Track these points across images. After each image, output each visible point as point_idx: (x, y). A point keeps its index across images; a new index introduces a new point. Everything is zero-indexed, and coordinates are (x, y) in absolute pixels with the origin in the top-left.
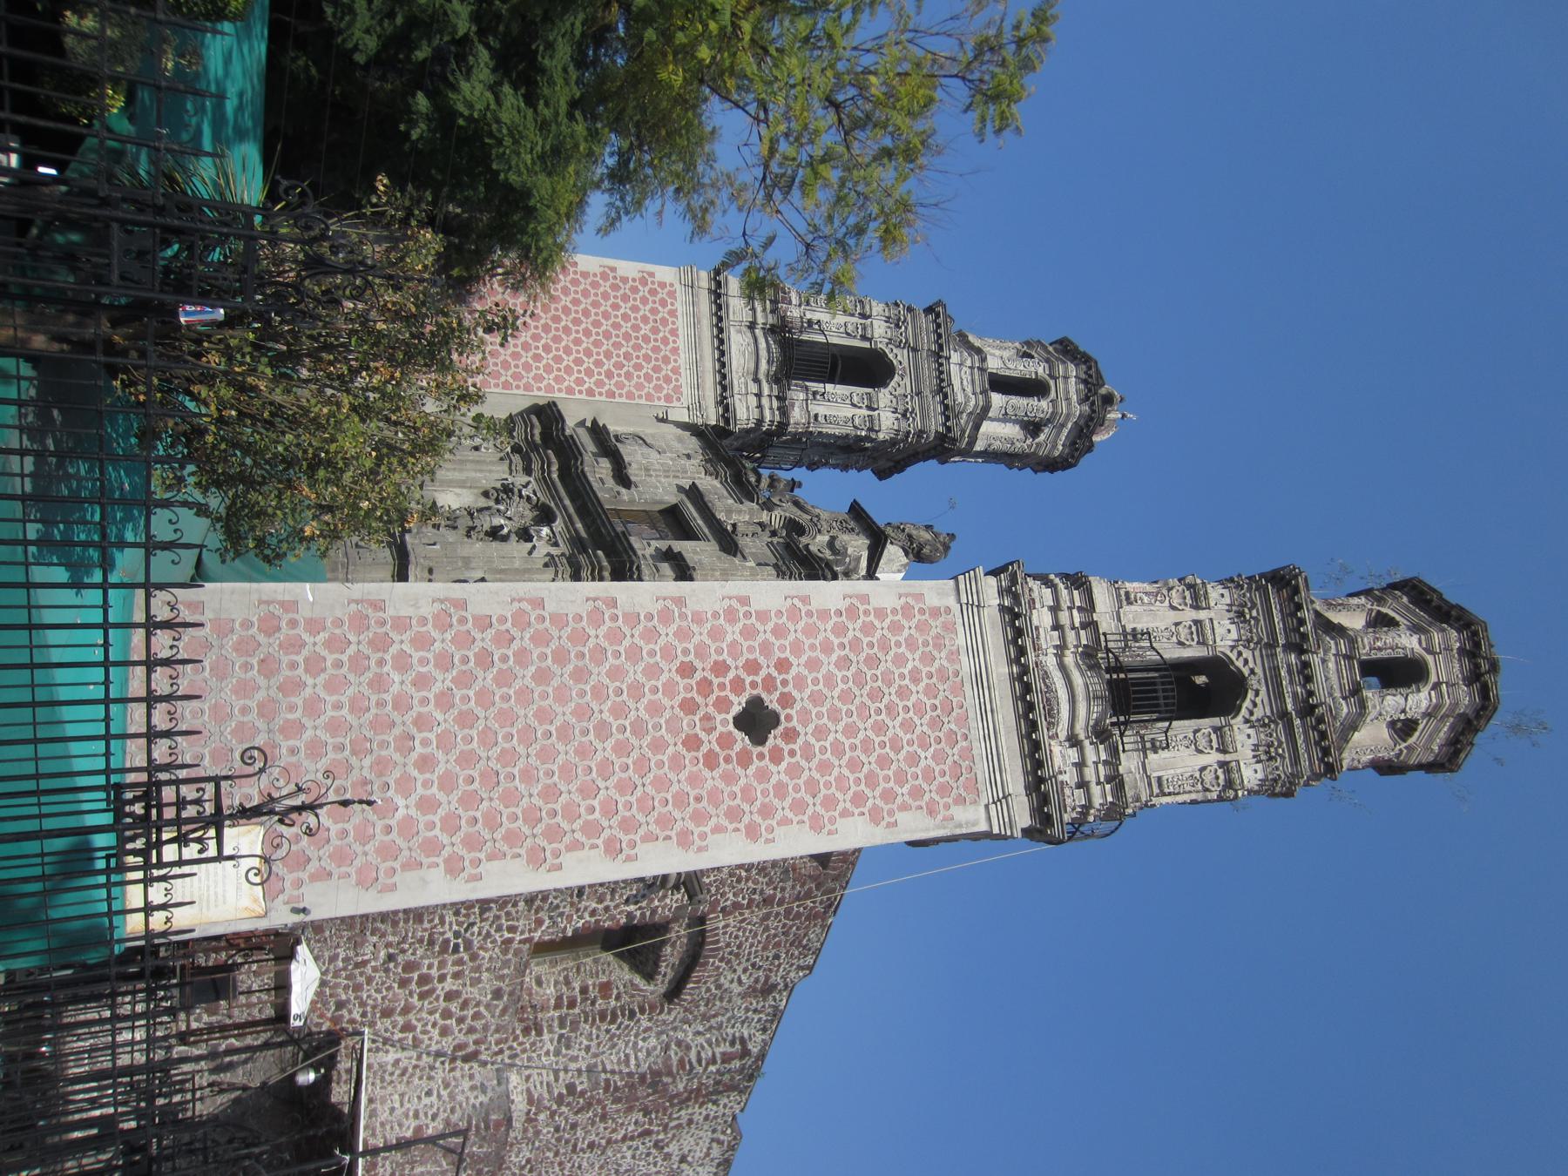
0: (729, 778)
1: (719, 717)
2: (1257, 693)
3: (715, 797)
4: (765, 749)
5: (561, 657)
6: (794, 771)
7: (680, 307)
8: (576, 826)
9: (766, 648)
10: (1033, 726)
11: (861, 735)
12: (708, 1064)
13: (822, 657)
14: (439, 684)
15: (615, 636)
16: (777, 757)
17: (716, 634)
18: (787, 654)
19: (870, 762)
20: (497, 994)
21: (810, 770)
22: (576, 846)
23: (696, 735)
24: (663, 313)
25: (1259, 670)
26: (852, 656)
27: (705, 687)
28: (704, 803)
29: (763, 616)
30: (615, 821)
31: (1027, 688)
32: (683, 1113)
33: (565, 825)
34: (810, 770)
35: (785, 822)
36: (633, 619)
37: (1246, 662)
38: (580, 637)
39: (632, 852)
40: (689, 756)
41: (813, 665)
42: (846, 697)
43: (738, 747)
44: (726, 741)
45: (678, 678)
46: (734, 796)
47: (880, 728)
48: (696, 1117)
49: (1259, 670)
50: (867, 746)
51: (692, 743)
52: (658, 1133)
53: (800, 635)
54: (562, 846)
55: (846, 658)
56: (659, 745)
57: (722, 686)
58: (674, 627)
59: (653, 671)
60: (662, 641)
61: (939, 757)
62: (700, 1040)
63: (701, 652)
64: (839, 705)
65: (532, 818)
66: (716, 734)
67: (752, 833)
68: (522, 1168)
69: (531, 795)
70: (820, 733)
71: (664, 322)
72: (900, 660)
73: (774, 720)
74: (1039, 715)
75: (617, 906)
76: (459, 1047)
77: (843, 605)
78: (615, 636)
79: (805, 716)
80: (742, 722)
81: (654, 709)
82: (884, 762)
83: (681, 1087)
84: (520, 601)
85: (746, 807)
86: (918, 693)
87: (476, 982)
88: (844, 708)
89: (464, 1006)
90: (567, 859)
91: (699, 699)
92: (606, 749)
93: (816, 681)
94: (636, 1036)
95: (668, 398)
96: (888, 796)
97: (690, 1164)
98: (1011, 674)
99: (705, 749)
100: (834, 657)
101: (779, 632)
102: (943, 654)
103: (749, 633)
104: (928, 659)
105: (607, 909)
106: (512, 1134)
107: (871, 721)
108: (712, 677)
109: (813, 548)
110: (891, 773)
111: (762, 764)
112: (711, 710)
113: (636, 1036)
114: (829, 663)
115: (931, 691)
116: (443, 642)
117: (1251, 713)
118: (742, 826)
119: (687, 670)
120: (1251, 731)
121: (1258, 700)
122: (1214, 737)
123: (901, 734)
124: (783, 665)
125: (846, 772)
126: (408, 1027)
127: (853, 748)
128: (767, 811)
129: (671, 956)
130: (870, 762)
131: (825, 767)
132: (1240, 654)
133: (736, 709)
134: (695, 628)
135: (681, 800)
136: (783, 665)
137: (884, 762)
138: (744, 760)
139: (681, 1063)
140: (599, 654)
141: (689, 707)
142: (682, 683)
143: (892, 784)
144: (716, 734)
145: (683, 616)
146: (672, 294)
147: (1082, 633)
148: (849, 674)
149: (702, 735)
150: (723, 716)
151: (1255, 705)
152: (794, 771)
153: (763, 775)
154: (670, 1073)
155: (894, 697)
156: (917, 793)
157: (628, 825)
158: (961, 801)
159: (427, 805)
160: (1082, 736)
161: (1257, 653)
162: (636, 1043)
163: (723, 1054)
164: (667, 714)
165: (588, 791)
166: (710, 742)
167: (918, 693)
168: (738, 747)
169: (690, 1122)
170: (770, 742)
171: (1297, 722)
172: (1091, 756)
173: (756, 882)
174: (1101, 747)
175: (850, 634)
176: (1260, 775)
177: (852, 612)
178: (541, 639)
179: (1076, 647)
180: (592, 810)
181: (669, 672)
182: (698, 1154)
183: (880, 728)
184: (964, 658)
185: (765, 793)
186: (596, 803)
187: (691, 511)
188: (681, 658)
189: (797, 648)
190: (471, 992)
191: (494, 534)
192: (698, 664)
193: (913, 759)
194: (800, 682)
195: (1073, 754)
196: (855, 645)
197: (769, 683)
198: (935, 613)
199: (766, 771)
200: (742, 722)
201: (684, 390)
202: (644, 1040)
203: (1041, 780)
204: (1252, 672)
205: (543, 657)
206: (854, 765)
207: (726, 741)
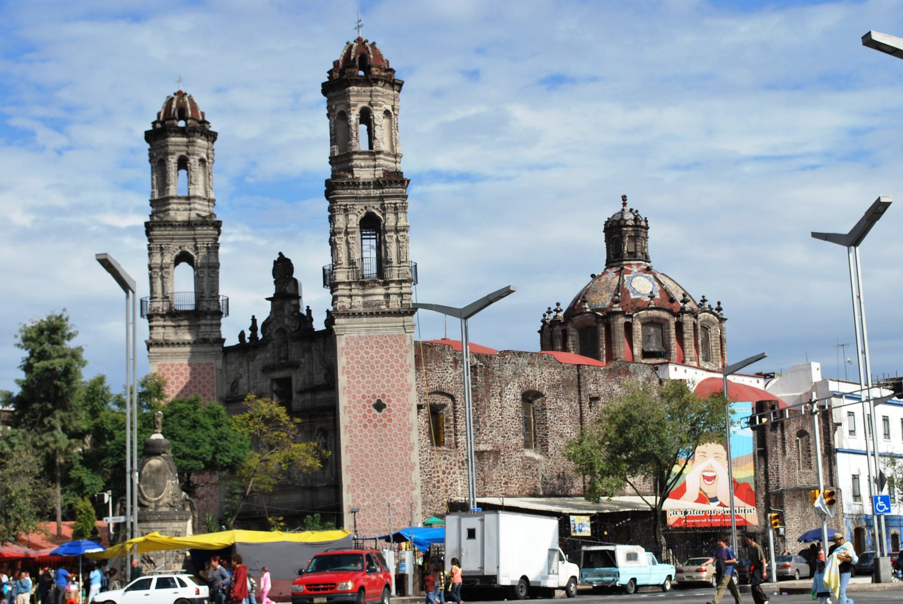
7: (169, 362)
9: (359, 402)
15: (356, 446)
16: (389, 401)
20: (445, 459)
21: (393, 391)
22: (410, 458)
24: (173, 370)
27: (370, 421)
29: (350, 402)
34: (393, 391)
35: (407, 400)
44: (385, 416)
50: (388, 372)
51: (385, 425)
56: (386, 435)
59: (366, 436)
63: (360, 422)
70: (383, 387)
71: (177, 370)
73: (379, 401)
76: (460, 468)
77: (346, 376)
79: (379, 391)
87: (440, 466)
89: (447, 468)
90: (413, 461)
92: (386, 450)
95: (212, 369)
109: (293, 330)
114: (363, 382)
119: (365, 426)
126: (451, 485)
128: (404, 405)
129: (439, 400)
131: (393, 386)
133: (376, 412)
138: (390, 411)
140: (361, 451)
146: (163, 365)
153: (394, 406)
157: (405, 444)
158: (405, 341)
159: (398, 495)
165: (397, 455)
166: (385, 420)
177: (348, 373)
181: (365, 431)
187: (278, 375)
190: (443, 467)
194: (369, 392)
198: (347, 343)
199: (393, 404)
201: (208, 361)
206: (393, 377)
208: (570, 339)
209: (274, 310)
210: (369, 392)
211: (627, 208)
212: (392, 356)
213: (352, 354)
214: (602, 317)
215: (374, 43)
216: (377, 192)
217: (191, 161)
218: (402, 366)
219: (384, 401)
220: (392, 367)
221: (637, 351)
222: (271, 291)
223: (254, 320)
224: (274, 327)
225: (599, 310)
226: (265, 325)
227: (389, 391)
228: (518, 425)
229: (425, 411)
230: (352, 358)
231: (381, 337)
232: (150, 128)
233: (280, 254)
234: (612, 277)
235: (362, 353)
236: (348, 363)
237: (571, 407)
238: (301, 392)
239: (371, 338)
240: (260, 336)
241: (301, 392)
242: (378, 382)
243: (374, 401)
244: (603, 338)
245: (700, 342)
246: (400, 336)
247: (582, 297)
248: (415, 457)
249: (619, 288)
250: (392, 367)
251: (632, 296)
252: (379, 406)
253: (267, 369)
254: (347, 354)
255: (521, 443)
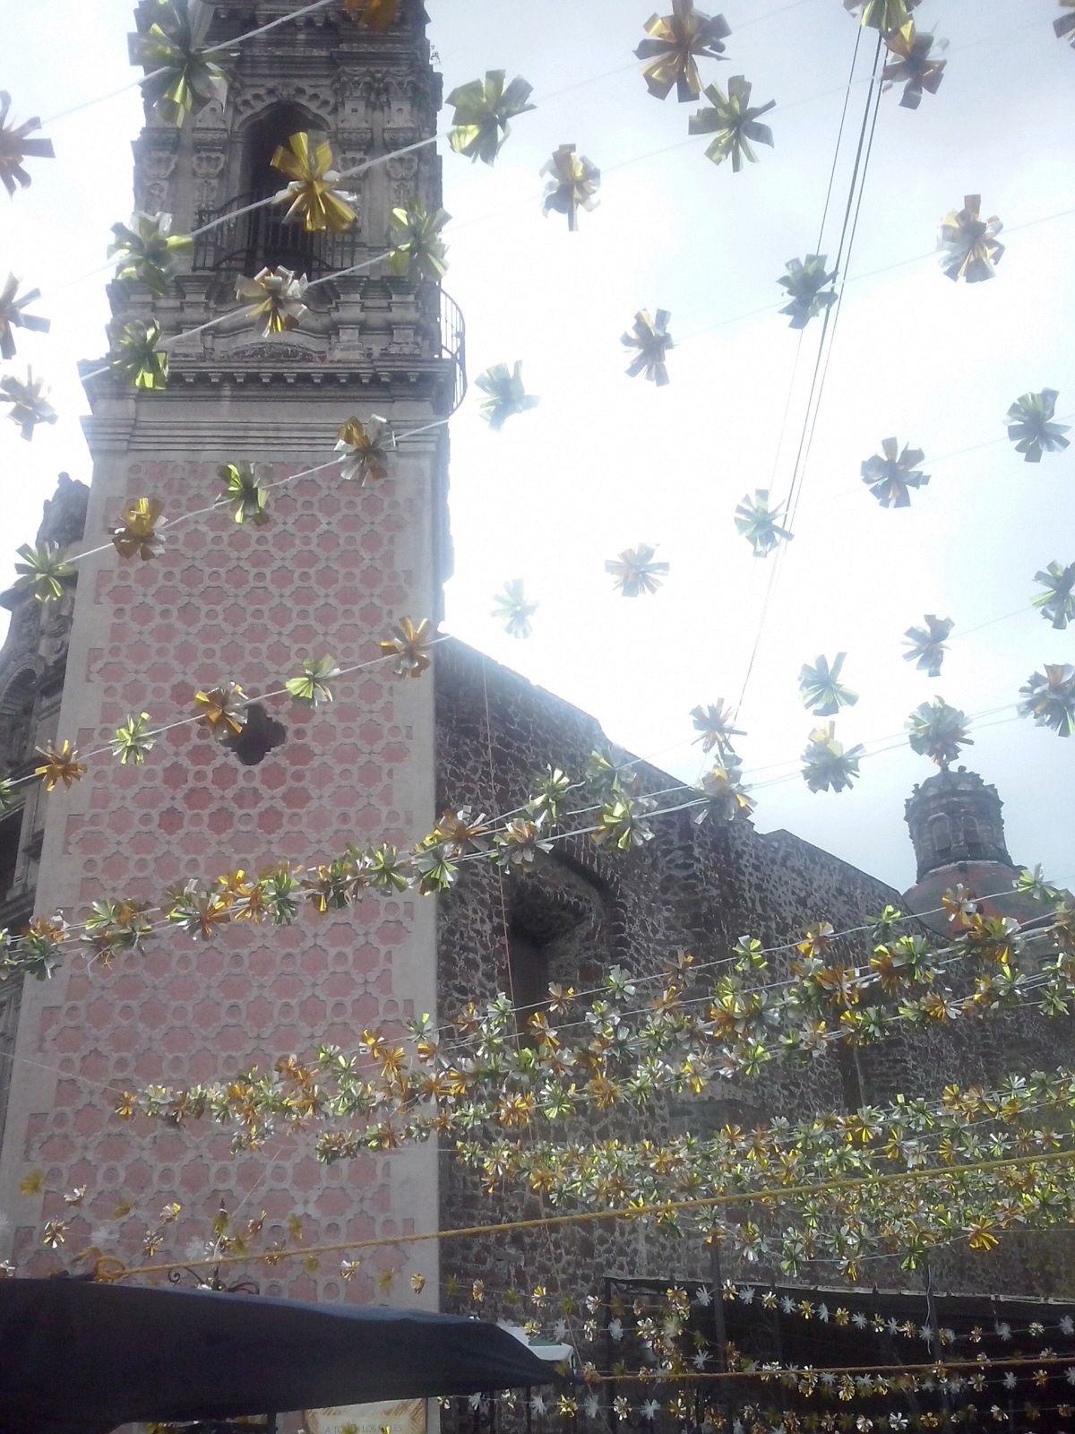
0: (323, 777)
1: (242, 783)
2: (300, 91)
4: (292, 728)
8: (359, 979)
10: (304, 379)
11: (289, 603)
12: (691, 856)
13: (177, 641)
14: (146, 1155)
18: (167, 686)
22: (385, 982)
23: (261, 815)
25: (271, 83)
26: (181, 602)
28: (352, 812)
30: (359, 928)
31: (253, 379)
32: (747, 895)
33: (357, 993)
35: (388, 712)
37: (257, 97)
39: (402, 907)
40: (286, 827)
41: (186, 654)
42: (234, 616)
43: (284, 762)
45: (181, 832)
46: (345, 773)
47: (283, 577)
48: (754, 880)
49: (271, 83)
50: (303, 596)
51: (270, 820)
52: (768, 927)
53: (143, 667)
54: (383, 1000)
55: (183, 610)
57: (200, 776)
58: (109, 832)
60: (126, 851)
62: (662, 863)
64: (245, 626)
66: (263, 790)
67: (396, 754)
68: (792, 1094)
69: (312, 1037)
74: (291, 371)
75: (485, 946)
82: (327, 578)
83: (715, 892)
84: (42, 1039)
85: (362, 760)
88: (250, 620)
90: (400, 992)
91: (213, 807)
93: (210, 653)
94: (649, 940)
97: (809, 895)
98: (234, 399)
99: (280, 805)
100: (180, 625)
102: (194, 483)
105: (486, 959)
106: (750, 1102)
107: (272, 588)
108: (186, 788)
110: (343, 571)
111: (309, 732)
112: (230, 793)
113: (649, 940)
117: (326, 103)
118: (386, 767)
119: (171, 820)
120: (349, 106)
121: (310, 91)
122: (349, 155)
123: (293, 551)
125: (334, 627)
127: (303, 614)
128: (371, 734)
132: (246, 103)
133: (233, 759)
134: (113, 806)
137: (327, 578)
139: (685, 888)
141: (221, 820)
142: (187, 828)
143: (357, 572)
144: (263, 790)
145: (94, 820)
147: (189, 298)
148: (205, 609)
149: (262, 806)
150: (240, 777)
151: (315, 96)
154: (697, 904)
155: (245, 555)
160: (325, 320)
161: (248, 81)
162: (659, 942)
163: (681, 837)
164: (229, 851)
168: (284, 762)
169: (759, 888)
170: (282, 720)
171: (344, 47)
172: (353, 313)
173: (475, 770)
174: (343, 298)
175: (150, 601)
176: (406, 107)
179: (207, 308)
180: (341, 957)
182: (798, 883)
184: (204, 456)
185: (347, 733)
186: (333, 951)
188: (153, 827)
189: (160, 673)
192: (165, 805)
195: (347, 336)
196: (165, 596)
202: (655, 931)
203: (375, 379)
204: (271, 92)
205: (126, 1011)
237: (964, 1059)
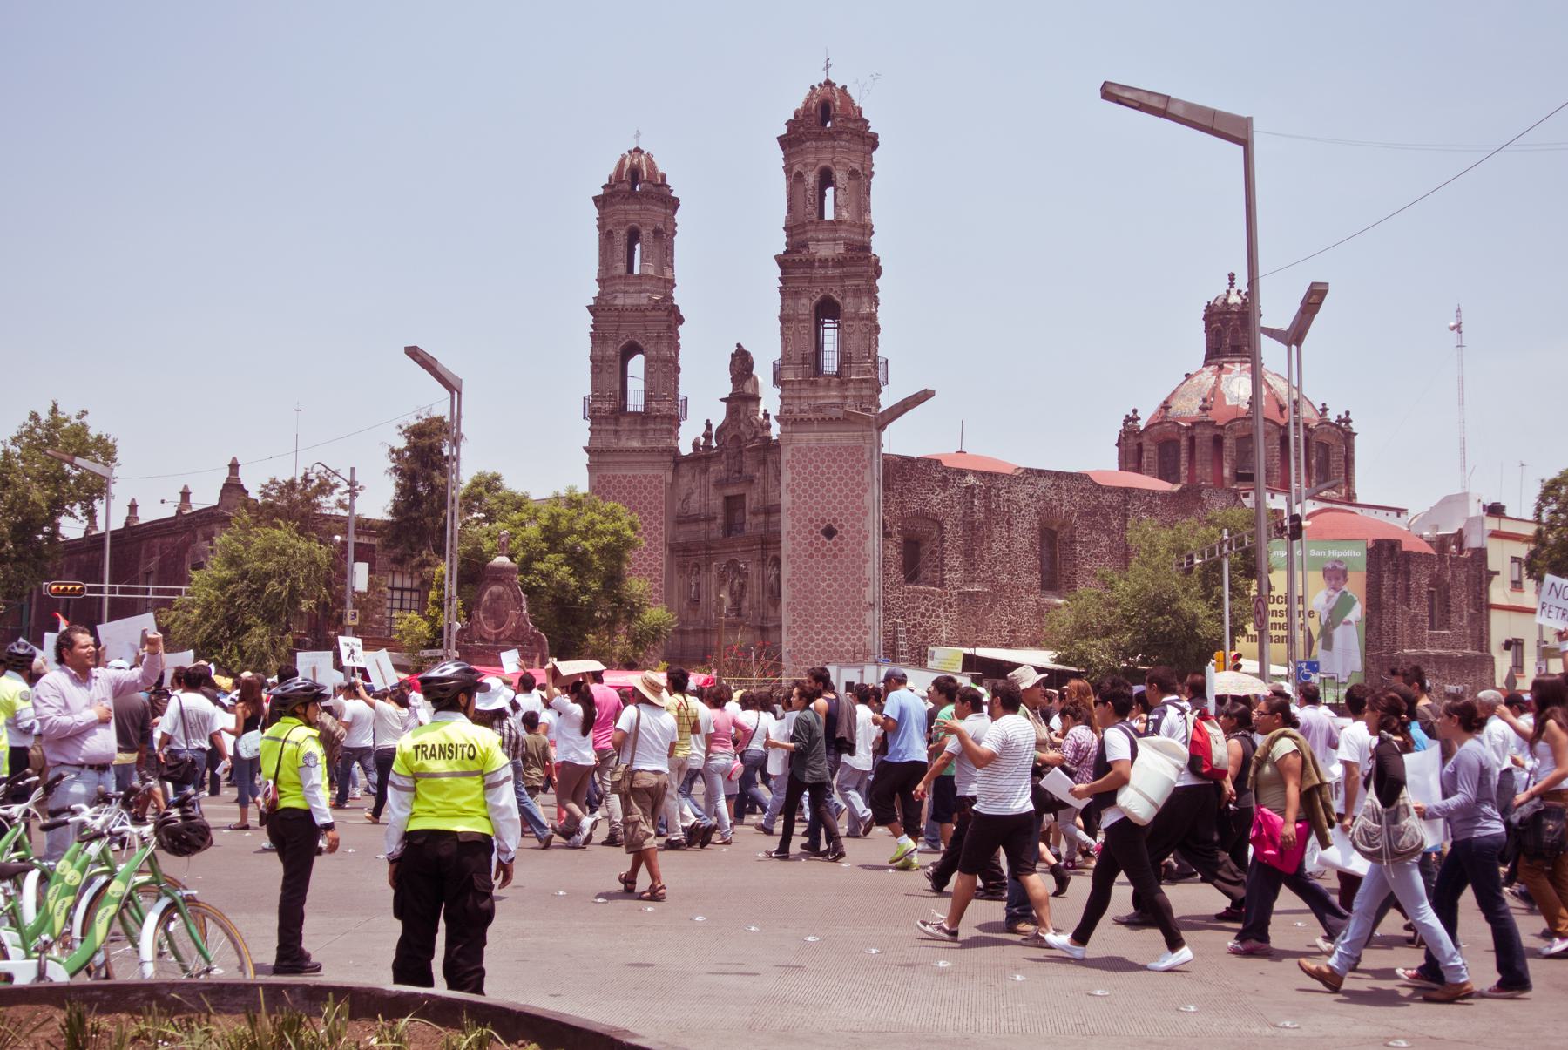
3: (853, 550)
5: (806, 598)
6: (847, 520)
9: (805, 526)
16: (842, 526)
17: (800, 544)
19: (846, 491)
24: (614, 482)
27: (817, 550)
36: (794, 574)
38: (800, 591)
42: (823, 497)
44: (835, 544)
50: (840, 491)
51: (835, 556)
56: (835, 568)
59: (811, 568)
61: (847, 461)
65: (854, 610)
72: (811, 473)
73: (829, 526)
78: (799, 580)
79: (829, 514)
80: (830, 538)
81: (824, 568)
86: (823, 467)
96: (858, 484)
101: (799, 521)
103: (799, 533)
104: (811, 461)
115: (823, 462)
116: (800, 633)
124: (811, 520)
130: (846, 491)
131: (847, 508)
135: (853, 562)
136: (811, 520)
138: (842, 538)
146: (604, 477)
152: (847, 520)
153: (848, 532)
156: (858, 473)
166: (835, 550)
167: (823, 467)
177: (793, 491)
178: (800, 604)
181: (812, 562)
183: (835, 485)
187: (730, 491)
189: (805, 515)
190: (922, 610)
191: (742, 586)
193: (846, 473)
194: (817, 515)
196: (805, 491)
197: (817, 526)
200: (830, 538)
206: (847, 497)
207: (835, 544)
208: (1145, 455)
209: (731, 412)
210: (817, 515)
211: (1234, 291)
212: (846, 473)
213: (799, 468)
214: (1187, 428)
215: (844, 87)
216: (837, 272)
217: (644, 232)
218: (858, 484)
219: (835, 526)
220: (846, 485)
221: (1226, 472)
222: (727, 389)
223: (709, 426)
224: (730, 434)
225: (1183, 419)
226: (719, 430)
227: (841, 514)
228: (1032, 561)
229: (898, 538)
230: (799, 473)
231: (834, 448)
232: (601, 192)
233: (739, 345)
234: (1208, 378)
235: (811, 468)
236: (793, 479)
238: (755, 513)
239: (822, 449)
240: (714, 444)
241: (755, 513)
242: (829, 503)
243: (823, 526)
244: (1184, 455)
245: (1313, 461)
246: (859, 448)
247: (1166, 406)
248: (873, 592)
249: (1215, 390)
250: (846, 485)
251: (1228, 403)
252: (829, 532)
253: (719, 484)
254: (793, 468)
255: (1036, 583)
